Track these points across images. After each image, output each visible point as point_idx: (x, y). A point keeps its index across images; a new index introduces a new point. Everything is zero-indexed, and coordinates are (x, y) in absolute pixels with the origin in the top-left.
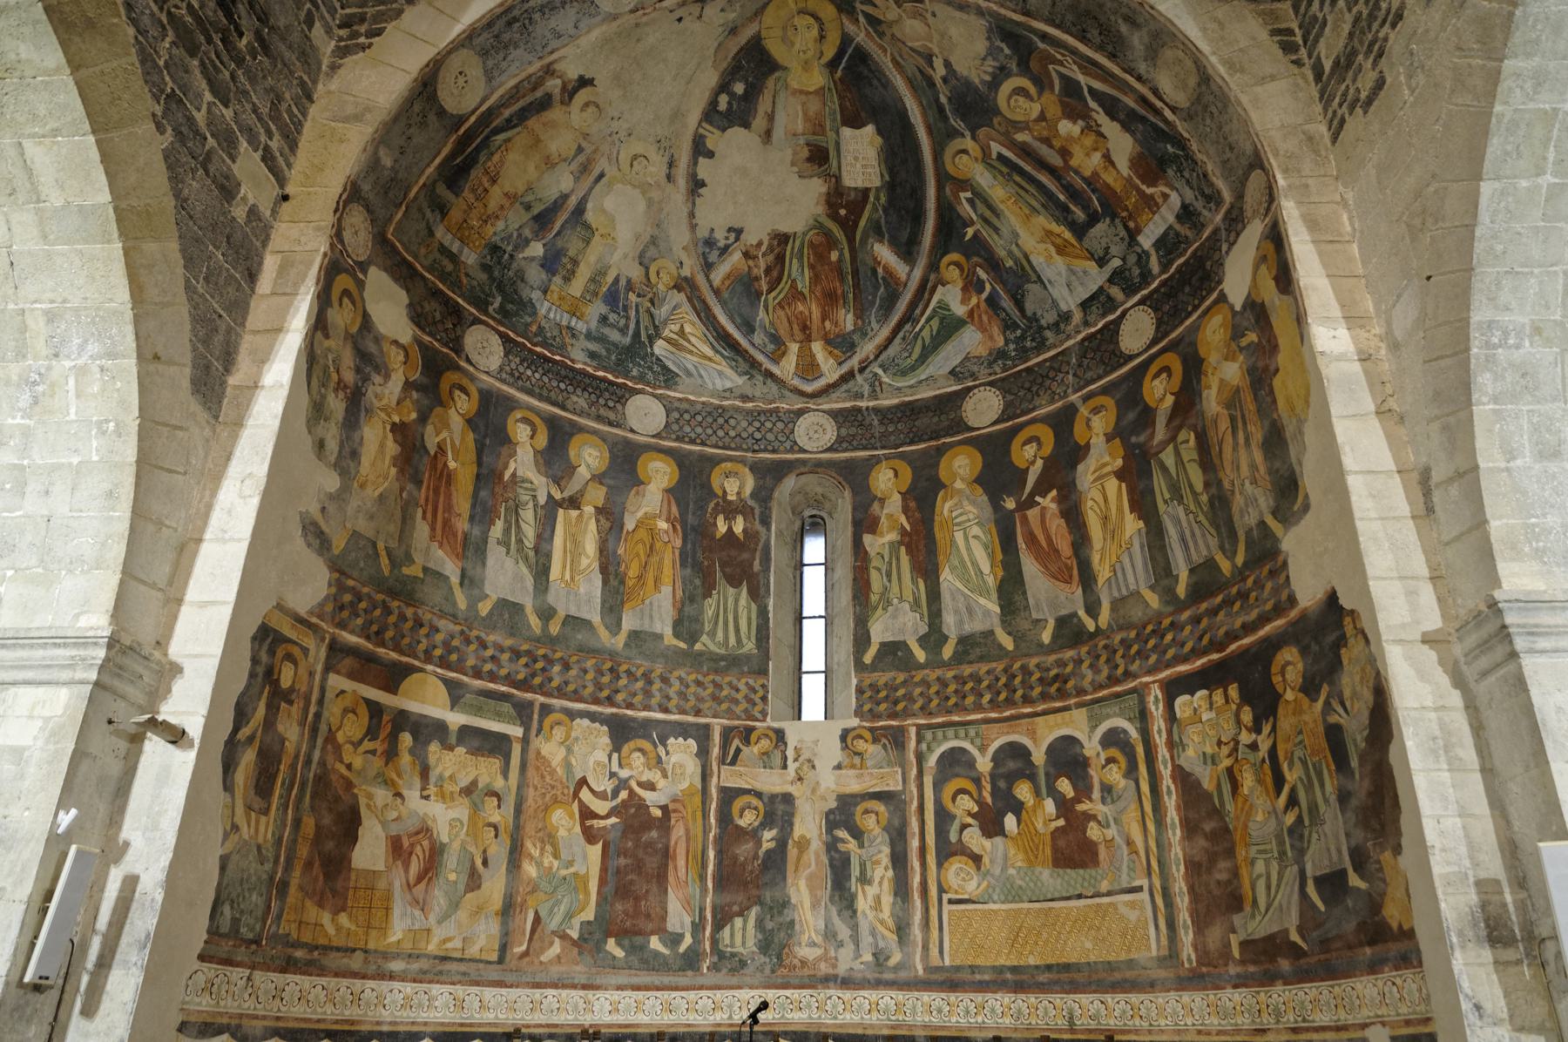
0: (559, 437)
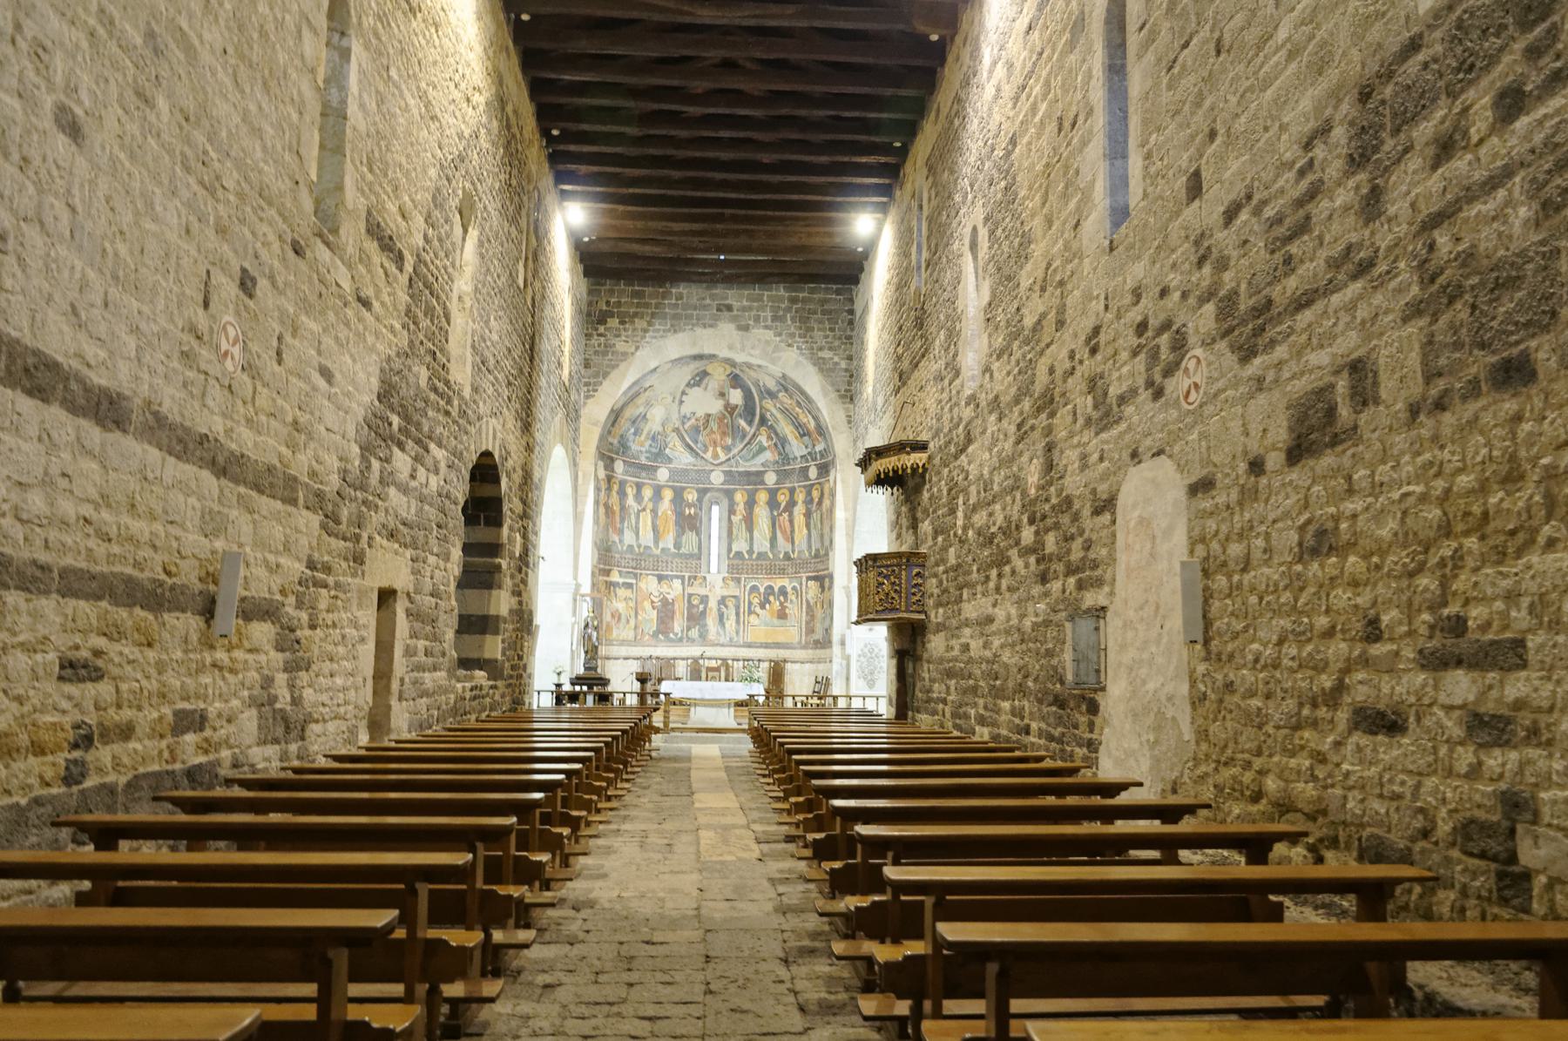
0: (639, 486)
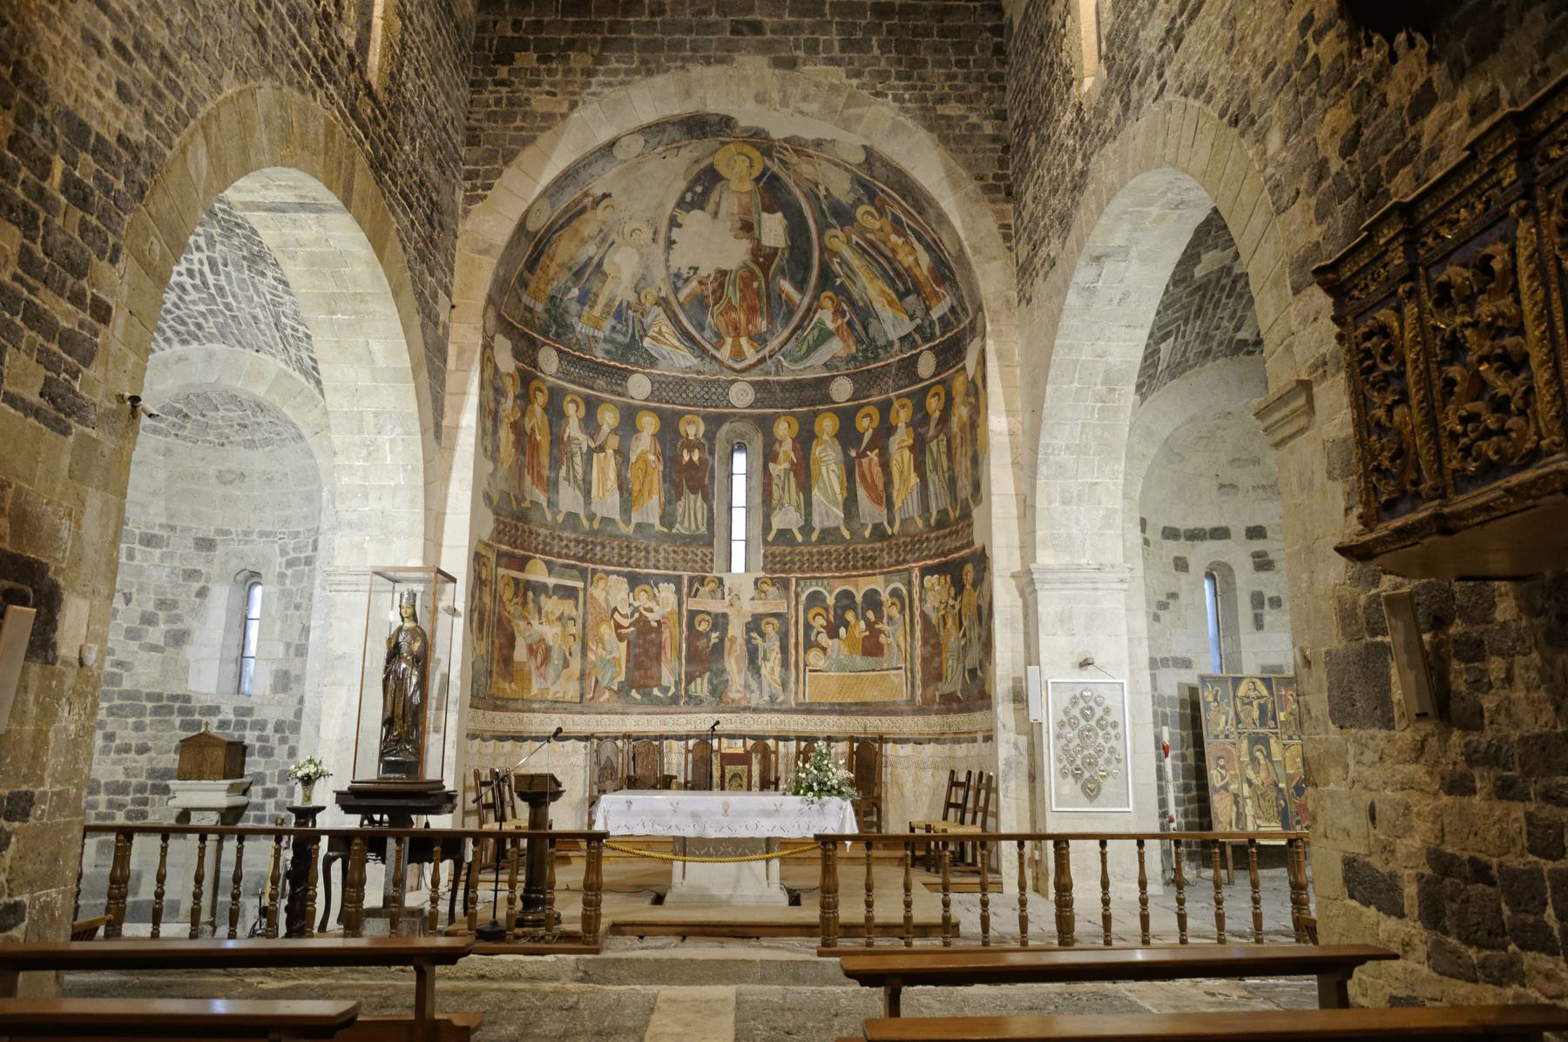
0: (592, 405)
